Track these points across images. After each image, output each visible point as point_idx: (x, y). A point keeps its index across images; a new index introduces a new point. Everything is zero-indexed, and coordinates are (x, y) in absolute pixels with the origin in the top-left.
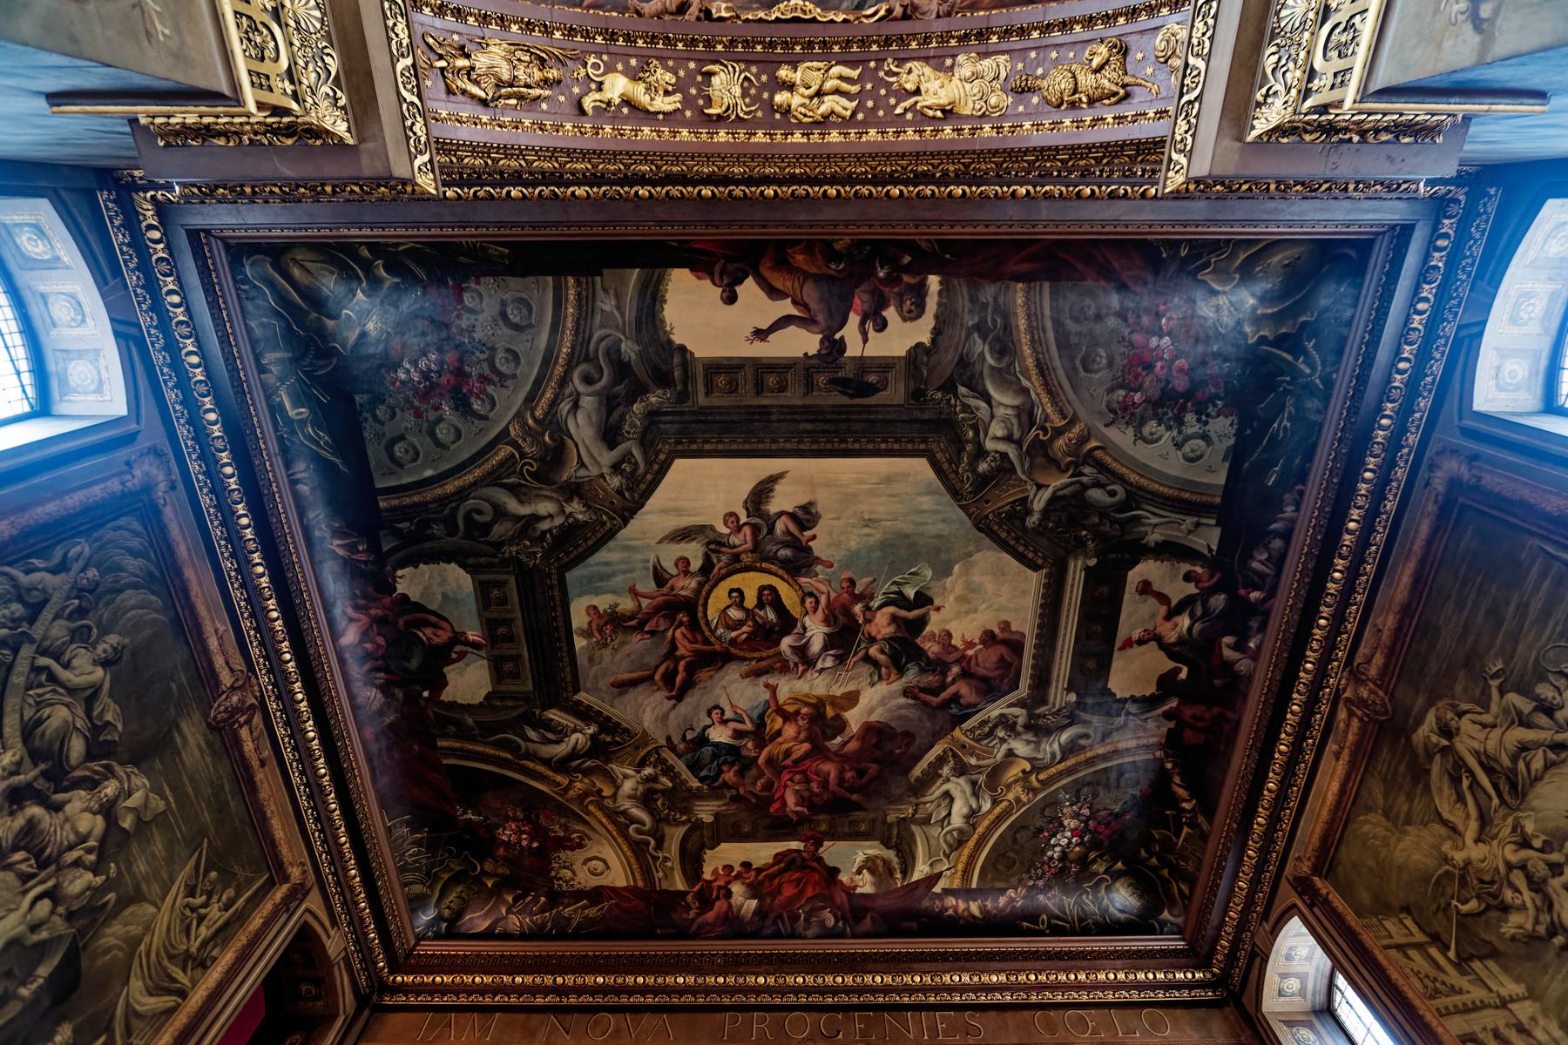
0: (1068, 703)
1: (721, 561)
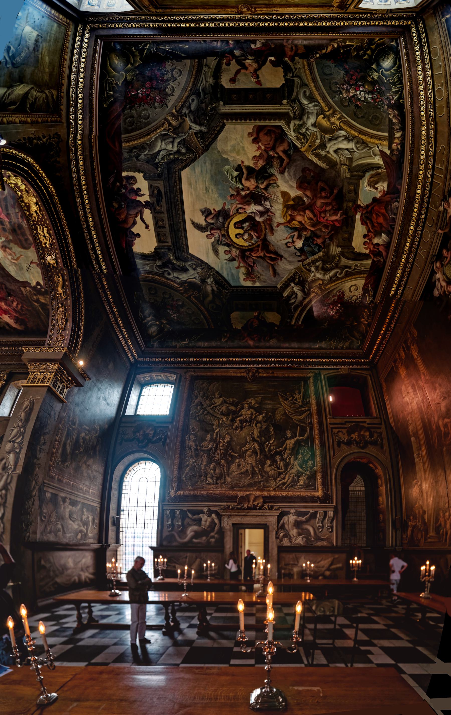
1: (225, 240)
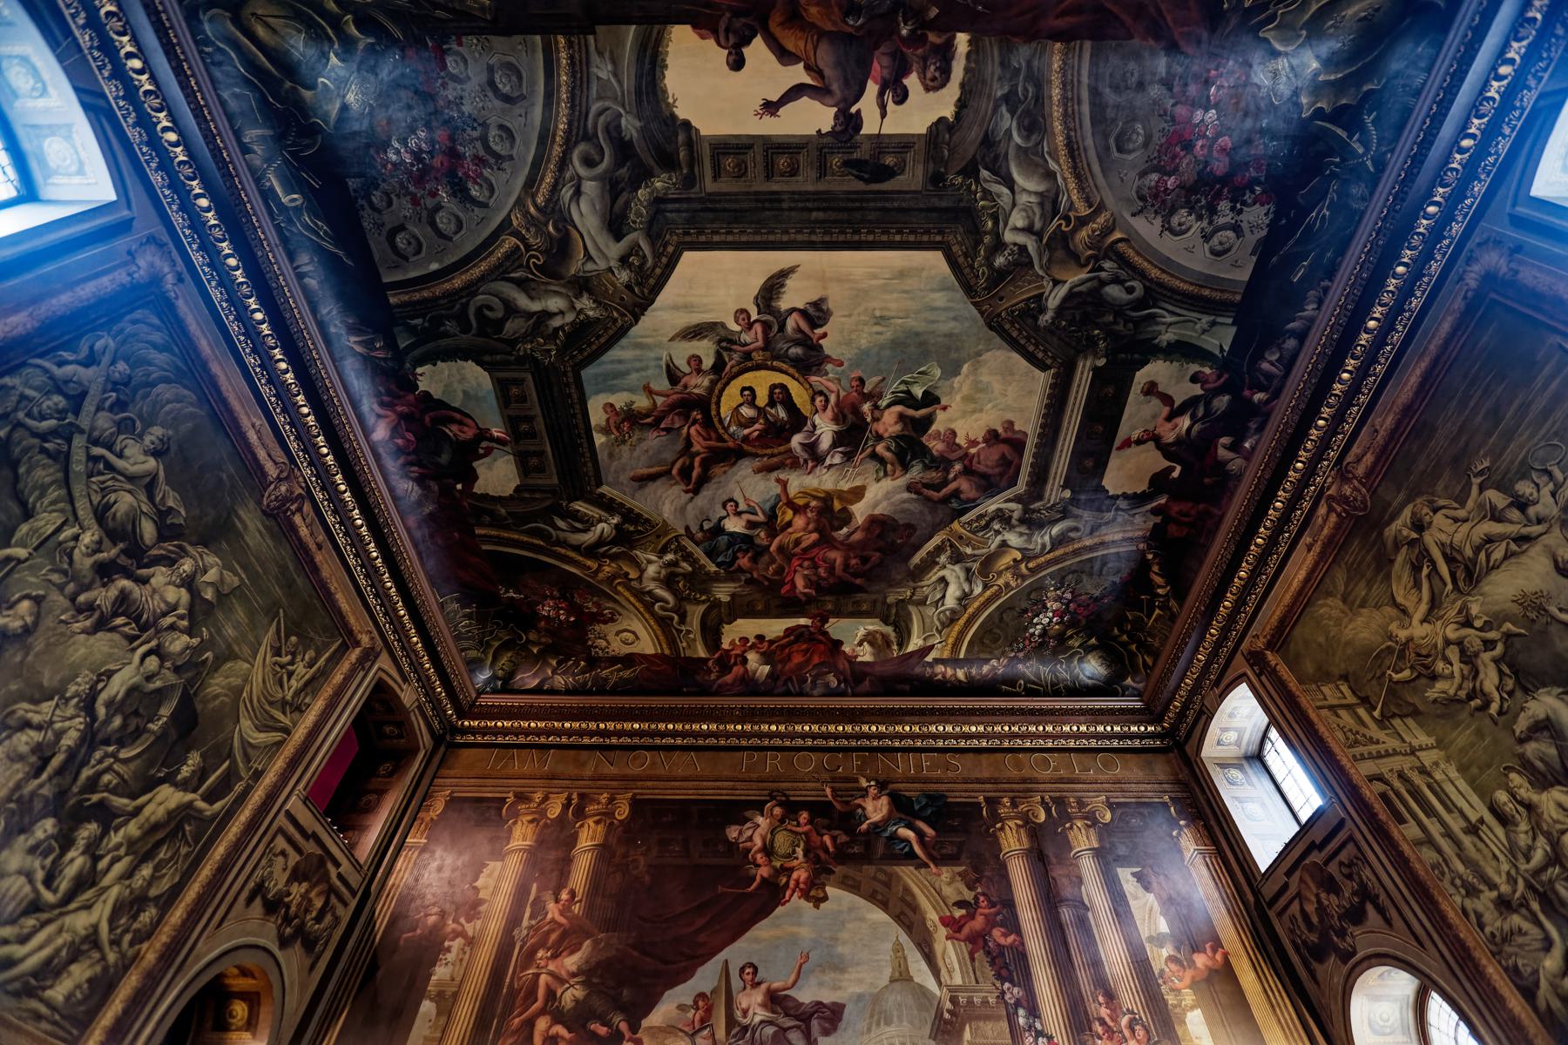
0: (1062, 499)
1: (732, 360)
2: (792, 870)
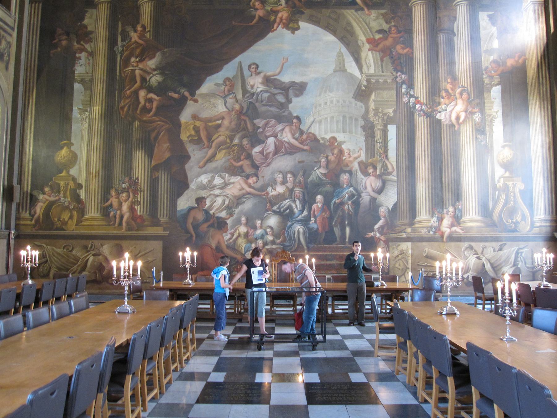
2: (277, 12)
